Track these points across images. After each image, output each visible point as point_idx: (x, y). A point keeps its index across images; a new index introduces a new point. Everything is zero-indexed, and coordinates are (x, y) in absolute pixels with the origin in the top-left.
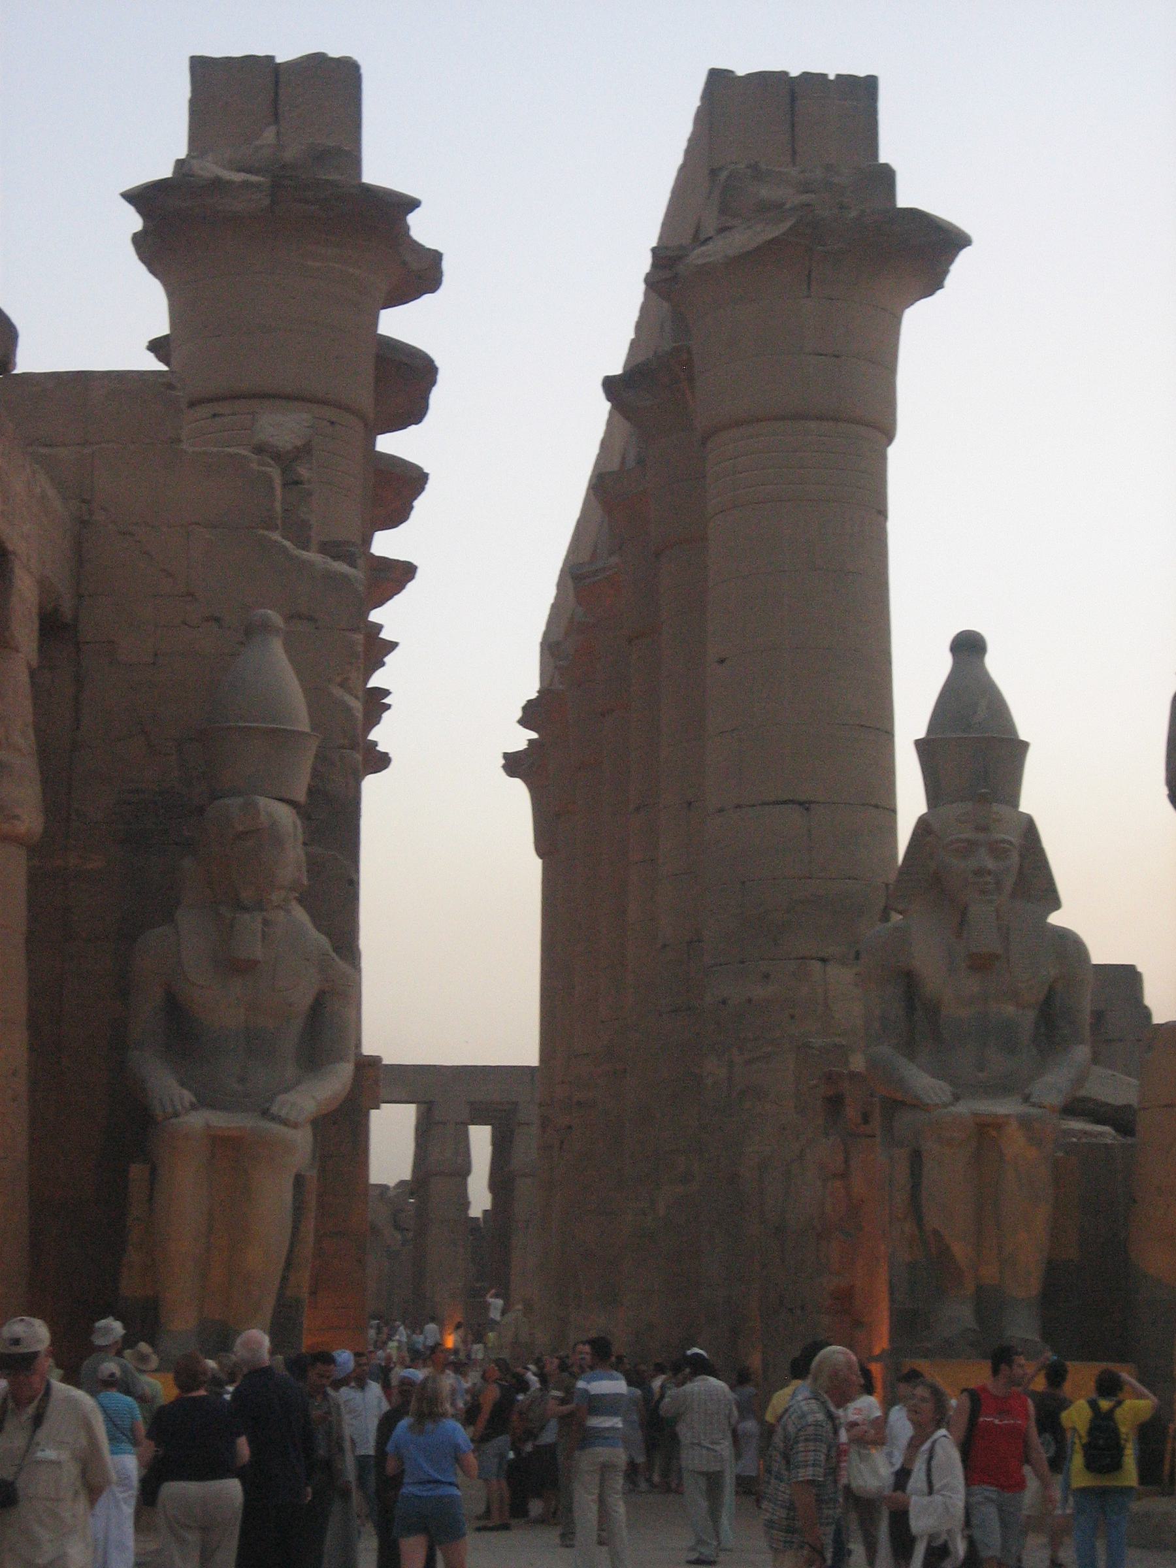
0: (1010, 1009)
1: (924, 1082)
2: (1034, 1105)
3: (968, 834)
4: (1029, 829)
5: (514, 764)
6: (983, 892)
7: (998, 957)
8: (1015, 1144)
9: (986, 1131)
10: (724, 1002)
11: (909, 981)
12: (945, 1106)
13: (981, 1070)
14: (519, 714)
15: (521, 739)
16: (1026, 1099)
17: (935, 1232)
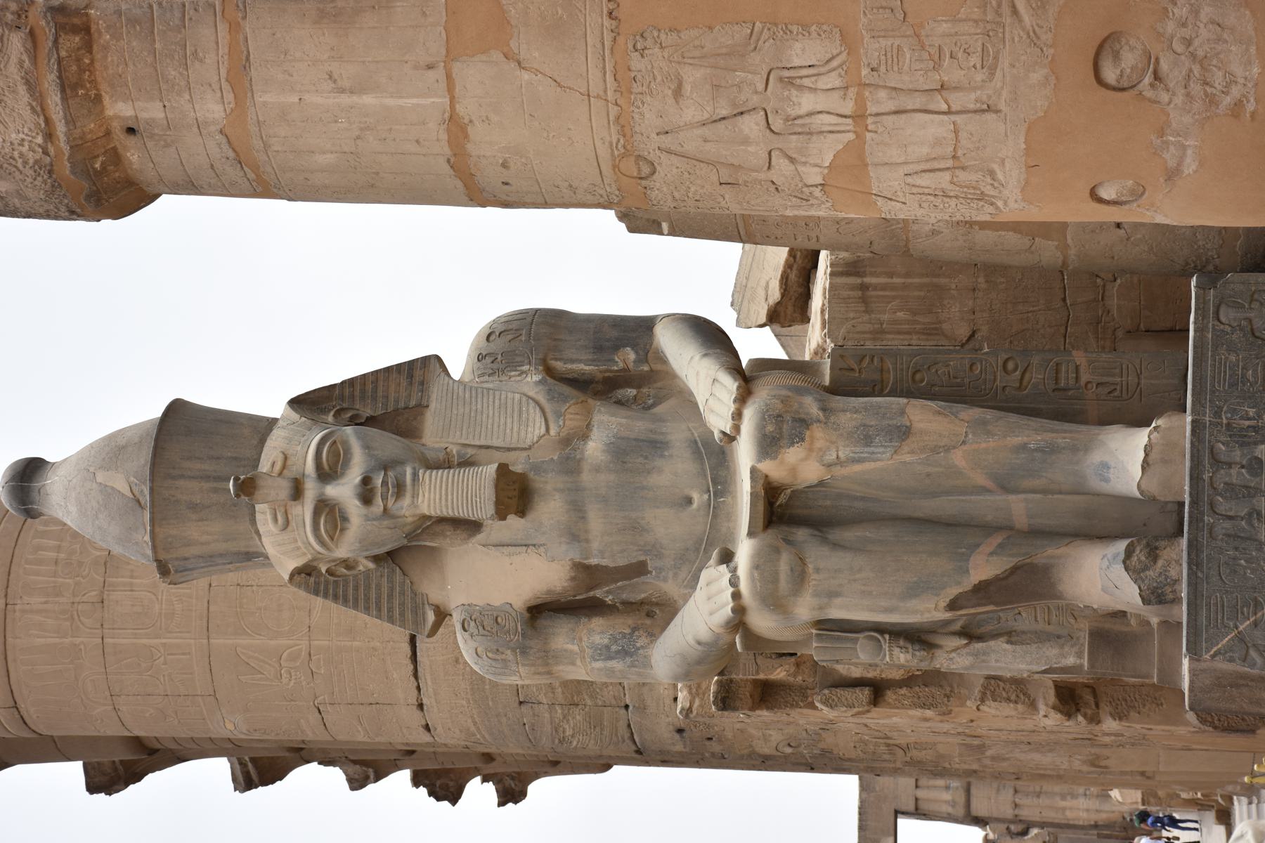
0: (594, 448)
1: (705, 609)
2: (737, 428)
3: (305, 511)
4: (309, 404)
5: (511, 793)
6: (400, 489)
7: (503, 470)
8: (802, 466)
9: (779, 510)
10: (680, 731)
11: (541, 612)
12: (734, 582)
13: (689, 501)
14: (446, 804)
15: (480, 792)
16: (730, 438)
17: (953, 605)
